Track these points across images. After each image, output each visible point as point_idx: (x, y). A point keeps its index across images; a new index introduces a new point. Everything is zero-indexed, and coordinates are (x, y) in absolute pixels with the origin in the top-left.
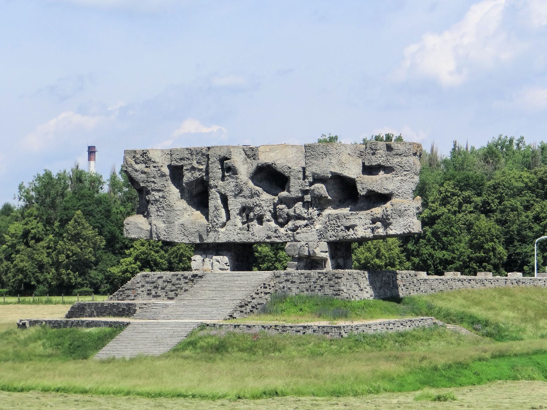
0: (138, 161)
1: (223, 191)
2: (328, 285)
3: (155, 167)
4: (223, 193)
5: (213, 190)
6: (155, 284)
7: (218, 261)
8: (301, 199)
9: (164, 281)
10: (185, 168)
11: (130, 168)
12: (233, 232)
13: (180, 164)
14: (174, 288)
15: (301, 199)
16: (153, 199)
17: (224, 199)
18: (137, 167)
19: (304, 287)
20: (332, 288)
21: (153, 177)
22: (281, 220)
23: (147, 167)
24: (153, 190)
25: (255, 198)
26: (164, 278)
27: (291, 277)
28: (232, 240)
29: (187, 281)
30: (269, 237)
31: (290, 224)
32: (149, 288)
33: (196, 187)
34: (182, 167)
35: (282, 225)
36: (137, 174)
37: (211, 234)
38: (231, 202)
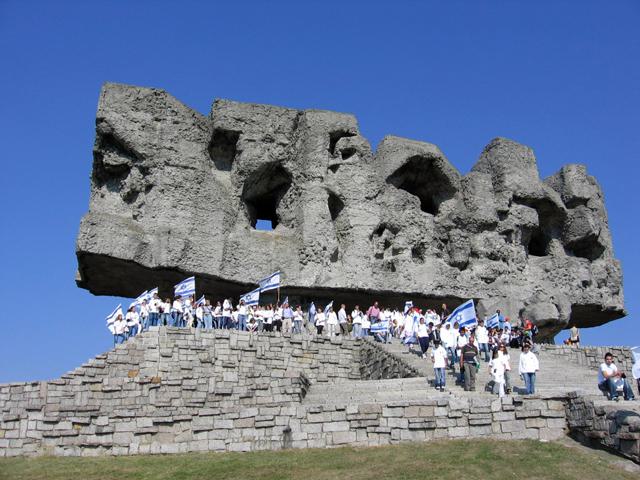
0: (140, 106)
1: (337, 190)
3: (176, 123)
4: (338, 193)
5: (316, 183)
6: (204, 356)
12: (356, 272)
13: (235, 129)
16: (168, 181)
17: (336, 204)
18: (134, 115)
21: (172, 140)
22: (460, 257)
23: (157, 120)
24: (167, 164)
25: (407, 211)
26: (233, 342)
28: (360, 285)
29: (297, 352)
31: (480, 267)
32: (185, 365)
34: (236, 135)
35: (463, 266)
36: (130, 127)
38: (358, 211)
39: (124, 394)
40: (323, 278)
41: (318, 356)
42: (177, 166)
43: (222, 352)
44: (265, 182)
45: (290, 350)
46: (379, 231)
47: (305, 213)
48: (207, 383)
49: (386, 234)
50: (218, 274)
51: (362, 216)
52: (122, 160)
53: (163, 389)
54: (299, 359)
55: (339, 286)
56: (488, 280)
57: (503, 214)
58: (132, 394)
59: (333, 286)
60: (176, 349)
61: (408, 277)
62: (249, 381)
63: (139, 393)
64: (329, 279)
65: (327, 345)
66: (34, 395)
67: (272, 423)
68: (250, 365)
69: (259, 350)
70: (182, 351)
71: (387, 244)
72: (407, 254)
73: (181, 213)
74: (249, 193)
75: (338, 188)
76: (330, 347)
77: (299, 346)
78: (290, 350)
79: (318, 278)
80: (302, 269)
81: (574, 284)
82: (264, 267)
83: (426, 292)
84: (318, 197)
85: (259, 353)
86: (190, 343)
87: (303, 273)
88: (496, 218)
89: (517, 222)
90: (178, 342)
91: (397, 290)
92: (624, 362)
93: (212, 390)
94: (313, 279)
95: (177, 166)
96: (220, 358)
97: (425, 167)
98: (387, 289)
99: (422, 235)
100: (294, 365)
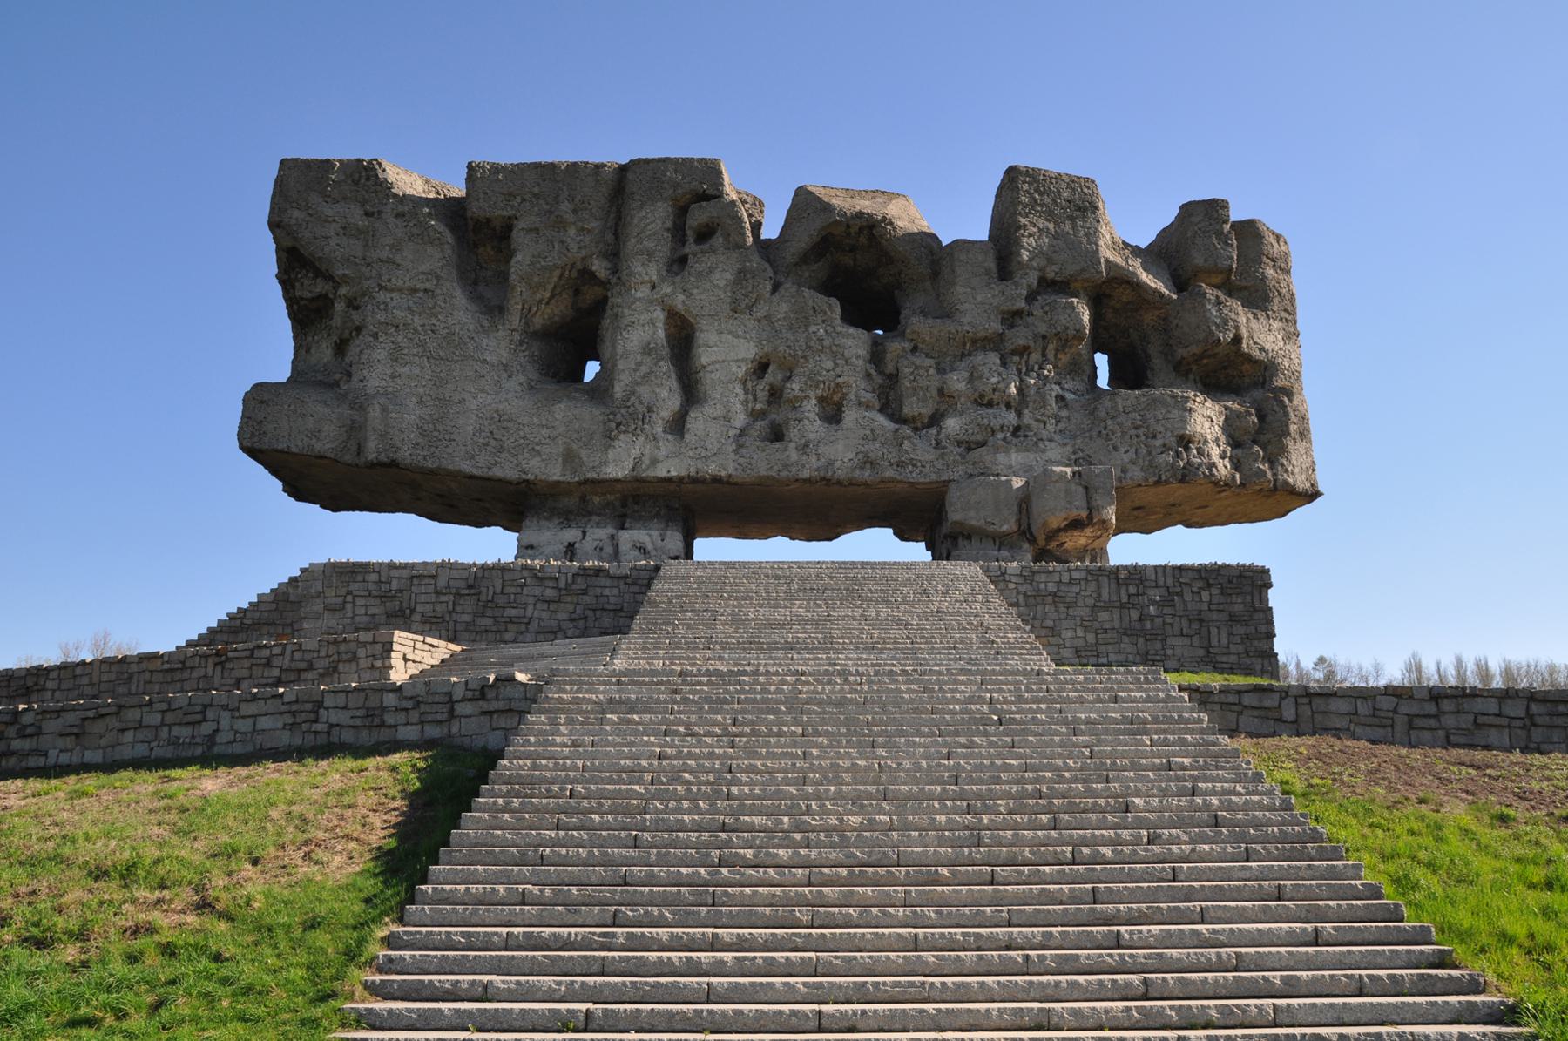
2: (1224, 617)
4: (680, 307)
7: (643, 550)
8: (992, 343)
9: (438, 593)
10: (521, 224)
11: (296, 213)
12: (714, 445)
14: (487, 622)
15: (992, 343)
19: (1117, 624)
20: (1240, 630)
26: (442, 582)
27: (1052, 587)
28: (712, 469)
29: (550, 593)
30: (868, 462)
33: (553, 296)
37: (623, 441)
39: (186, 675)
40: (647, 461)
41: (587, 599)
42: (400, 290)
43: (423, 598)
44: (566, 296)
45: (537, 591)
46: (761, 368)
47: (620, 350)
48: (283, 654)
49: (774, 375)
50: (467, 467)
51: (726, 352)
52: (321, 287)
53: (229, 665)
54: (552, 607)
55: (674, 473)
56: (969, 446)
57: (1012, 318)
58: (195, 674)
59: (662, 473)
60: (349, 598)
61: (803, 448)
62: (332, 649)
63: (202, 672)
64: (654, 462)
65: (602, 581)
66: (85, 680)
67: (199, 717)
68: (466, 618)
69: (484, 590)
70: (360, 601)
71: (775, 394)
72: (811, 407)
73: (405, 370)
74: (537, 322)
75: (681, 297)
76: (608, 582)
77: (551, 584)
78: (537, 591)
79: (638, 462)
80: (606, 448)
81: (1158, 442)
82: (545, 450)
83: (841, 474)
84: (644, 317)
85: (483, 598)
86: (372, 587)
87: (611, 455)
88: (996, 326)
89: (1042, 329)
90: (354, 587)
91: (784, 474)
92: (1205, 596)
93: (287, 663)
94: (629, 464)
95: (400, 290)
96: (419, 608)
97: (863, 239)
98: (763, 473)
99: (838, 370)
100: (545, 615)
